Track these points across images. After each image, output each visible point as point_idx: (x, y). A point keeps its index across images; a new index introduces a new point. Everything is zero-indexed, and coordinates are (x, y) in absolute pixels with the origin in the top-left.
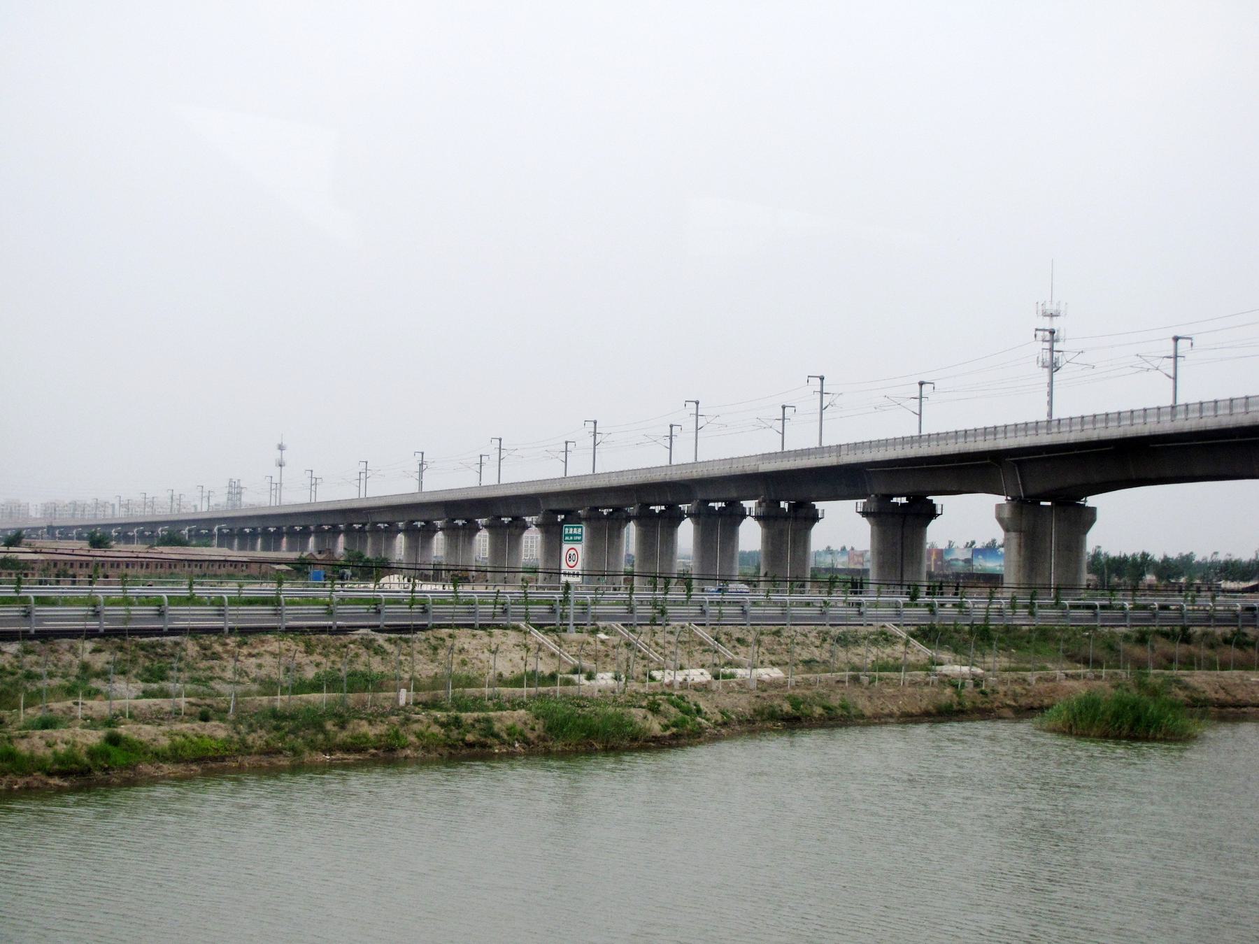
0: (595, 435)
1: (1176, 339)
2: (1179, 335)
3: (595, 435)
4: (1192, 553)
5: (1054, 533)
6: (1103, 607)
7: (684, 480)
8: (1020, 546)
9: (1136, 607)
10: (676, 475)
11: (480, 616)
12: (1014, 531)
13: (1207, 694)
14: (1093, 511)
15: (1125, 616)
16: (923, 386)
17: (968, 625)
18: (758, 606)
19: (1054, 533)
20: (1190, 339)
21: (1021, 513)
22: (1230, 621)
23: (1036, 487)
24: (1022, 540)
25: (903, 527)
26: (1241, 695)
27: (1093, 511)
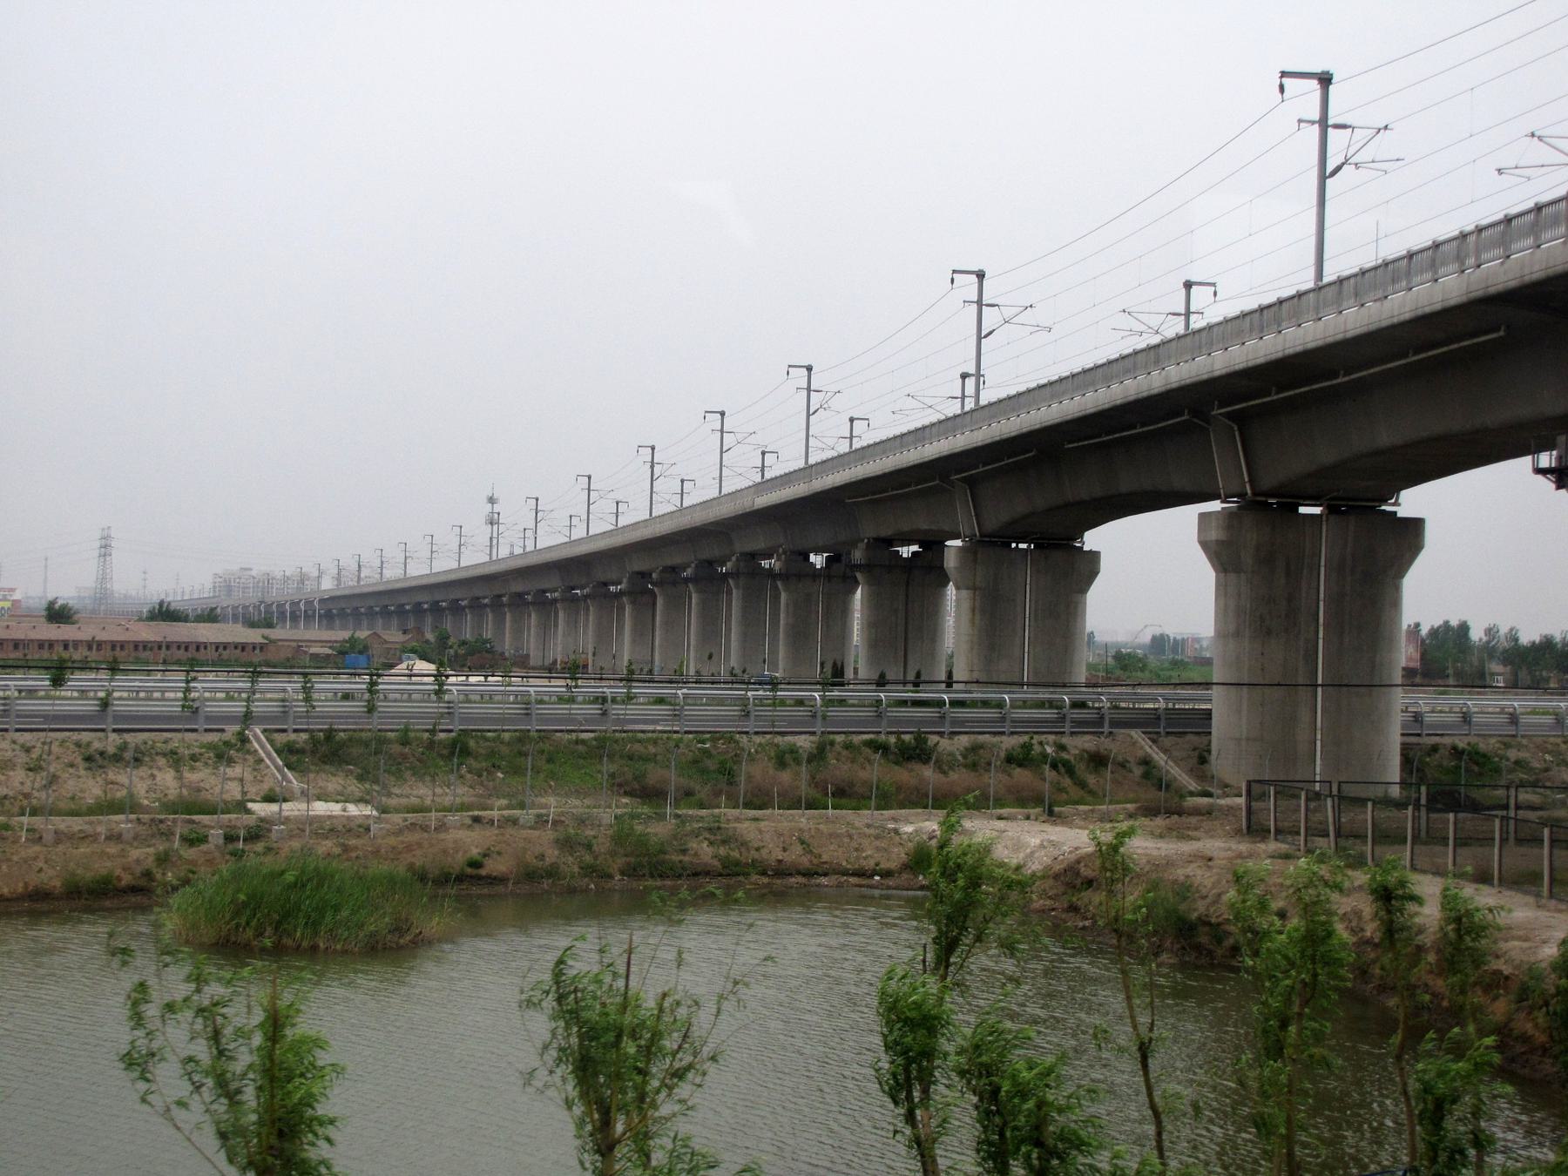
0: (652, 467)
1: (1188, 285)
2: (1193, 279)
3: (652, 467)
4: (1511, 630)
5: (1028, 587)
6: (954, 703)
7: (704, 525)
8: (973, 610)
9: (828, 702)
10: (699, 518)
11: (18, 716)
12: (968, 589)
13: (764, 852)
14: (1094, 556)
15: (1063, 719)
16: (967, 380)
17: (427, 731)
18: (845, 706)
19: (1028, 587)
20: (1214, 285)
21: (975, 561)
22: (998, 722)
23: (997, 518)
24: (977, 604)
25: (908, 584)
26: (831, 853)
27: (1094, 556)
